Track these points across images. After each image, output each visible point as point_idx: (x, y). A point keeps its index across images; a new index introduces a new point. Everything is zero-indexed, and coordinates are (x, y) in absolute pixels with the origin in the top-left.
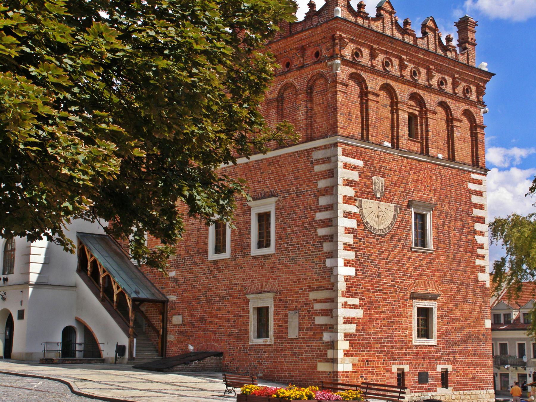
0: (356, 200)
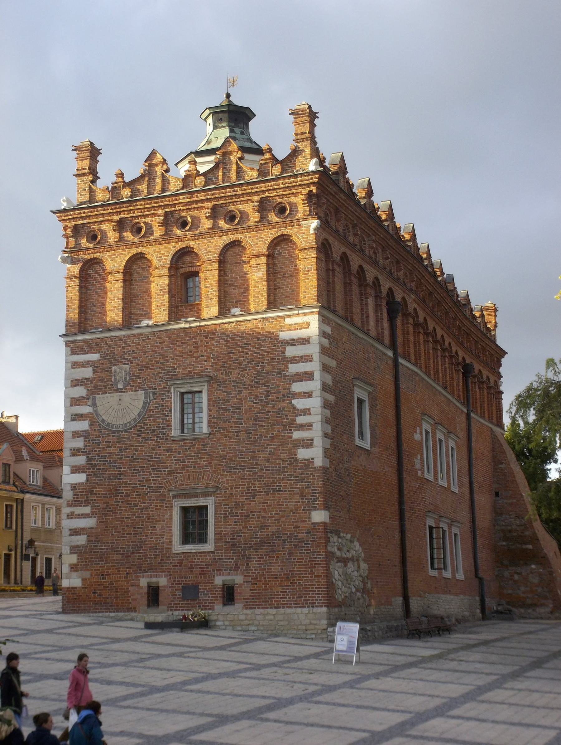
0: (88, 399)
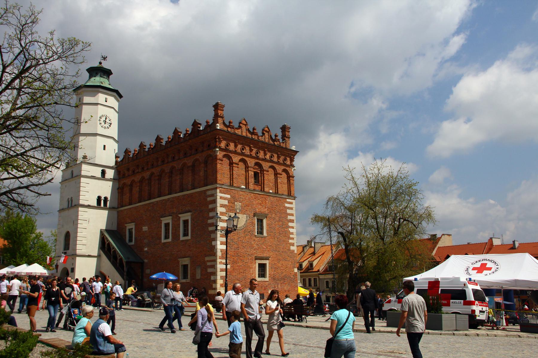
0: (226, 214)
